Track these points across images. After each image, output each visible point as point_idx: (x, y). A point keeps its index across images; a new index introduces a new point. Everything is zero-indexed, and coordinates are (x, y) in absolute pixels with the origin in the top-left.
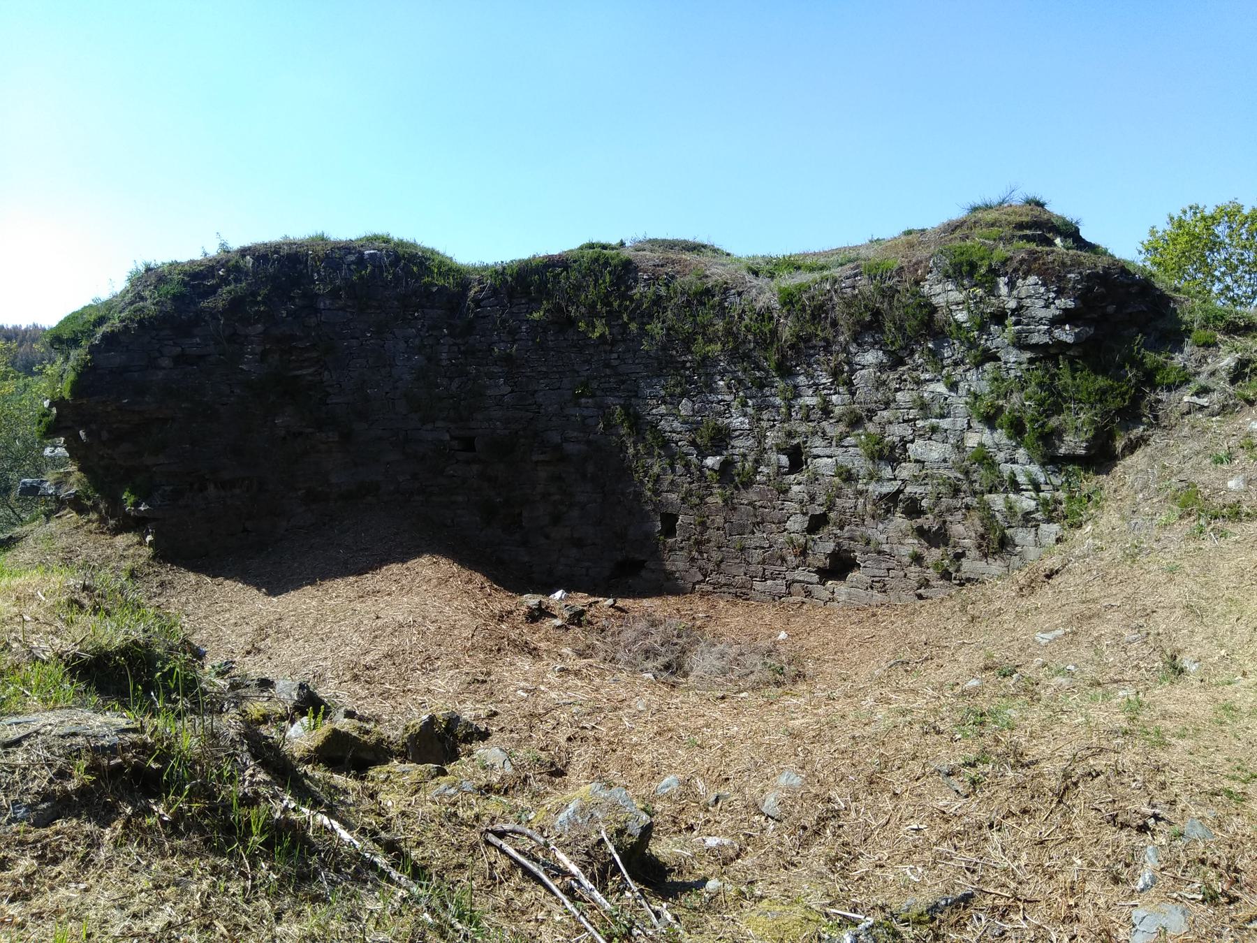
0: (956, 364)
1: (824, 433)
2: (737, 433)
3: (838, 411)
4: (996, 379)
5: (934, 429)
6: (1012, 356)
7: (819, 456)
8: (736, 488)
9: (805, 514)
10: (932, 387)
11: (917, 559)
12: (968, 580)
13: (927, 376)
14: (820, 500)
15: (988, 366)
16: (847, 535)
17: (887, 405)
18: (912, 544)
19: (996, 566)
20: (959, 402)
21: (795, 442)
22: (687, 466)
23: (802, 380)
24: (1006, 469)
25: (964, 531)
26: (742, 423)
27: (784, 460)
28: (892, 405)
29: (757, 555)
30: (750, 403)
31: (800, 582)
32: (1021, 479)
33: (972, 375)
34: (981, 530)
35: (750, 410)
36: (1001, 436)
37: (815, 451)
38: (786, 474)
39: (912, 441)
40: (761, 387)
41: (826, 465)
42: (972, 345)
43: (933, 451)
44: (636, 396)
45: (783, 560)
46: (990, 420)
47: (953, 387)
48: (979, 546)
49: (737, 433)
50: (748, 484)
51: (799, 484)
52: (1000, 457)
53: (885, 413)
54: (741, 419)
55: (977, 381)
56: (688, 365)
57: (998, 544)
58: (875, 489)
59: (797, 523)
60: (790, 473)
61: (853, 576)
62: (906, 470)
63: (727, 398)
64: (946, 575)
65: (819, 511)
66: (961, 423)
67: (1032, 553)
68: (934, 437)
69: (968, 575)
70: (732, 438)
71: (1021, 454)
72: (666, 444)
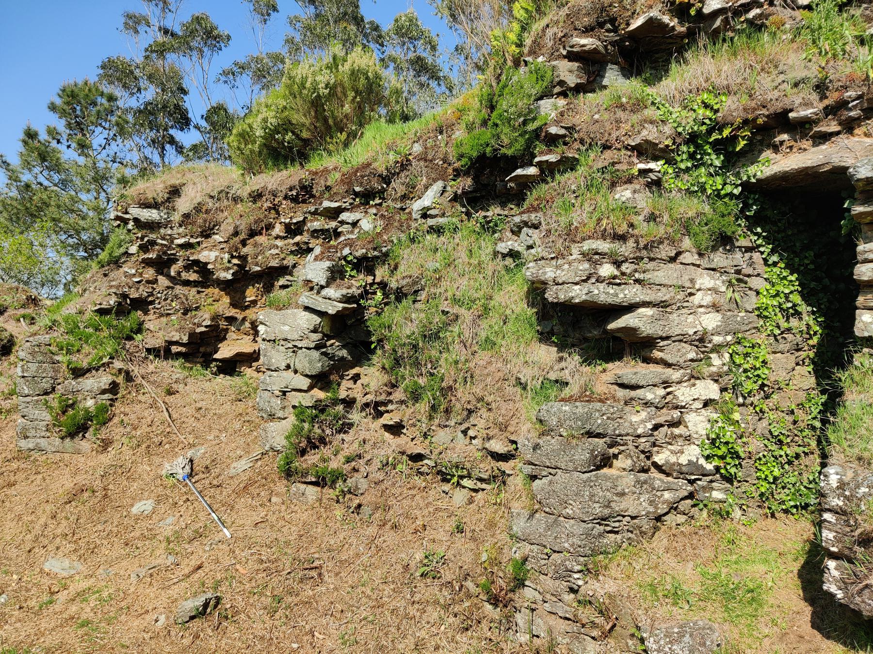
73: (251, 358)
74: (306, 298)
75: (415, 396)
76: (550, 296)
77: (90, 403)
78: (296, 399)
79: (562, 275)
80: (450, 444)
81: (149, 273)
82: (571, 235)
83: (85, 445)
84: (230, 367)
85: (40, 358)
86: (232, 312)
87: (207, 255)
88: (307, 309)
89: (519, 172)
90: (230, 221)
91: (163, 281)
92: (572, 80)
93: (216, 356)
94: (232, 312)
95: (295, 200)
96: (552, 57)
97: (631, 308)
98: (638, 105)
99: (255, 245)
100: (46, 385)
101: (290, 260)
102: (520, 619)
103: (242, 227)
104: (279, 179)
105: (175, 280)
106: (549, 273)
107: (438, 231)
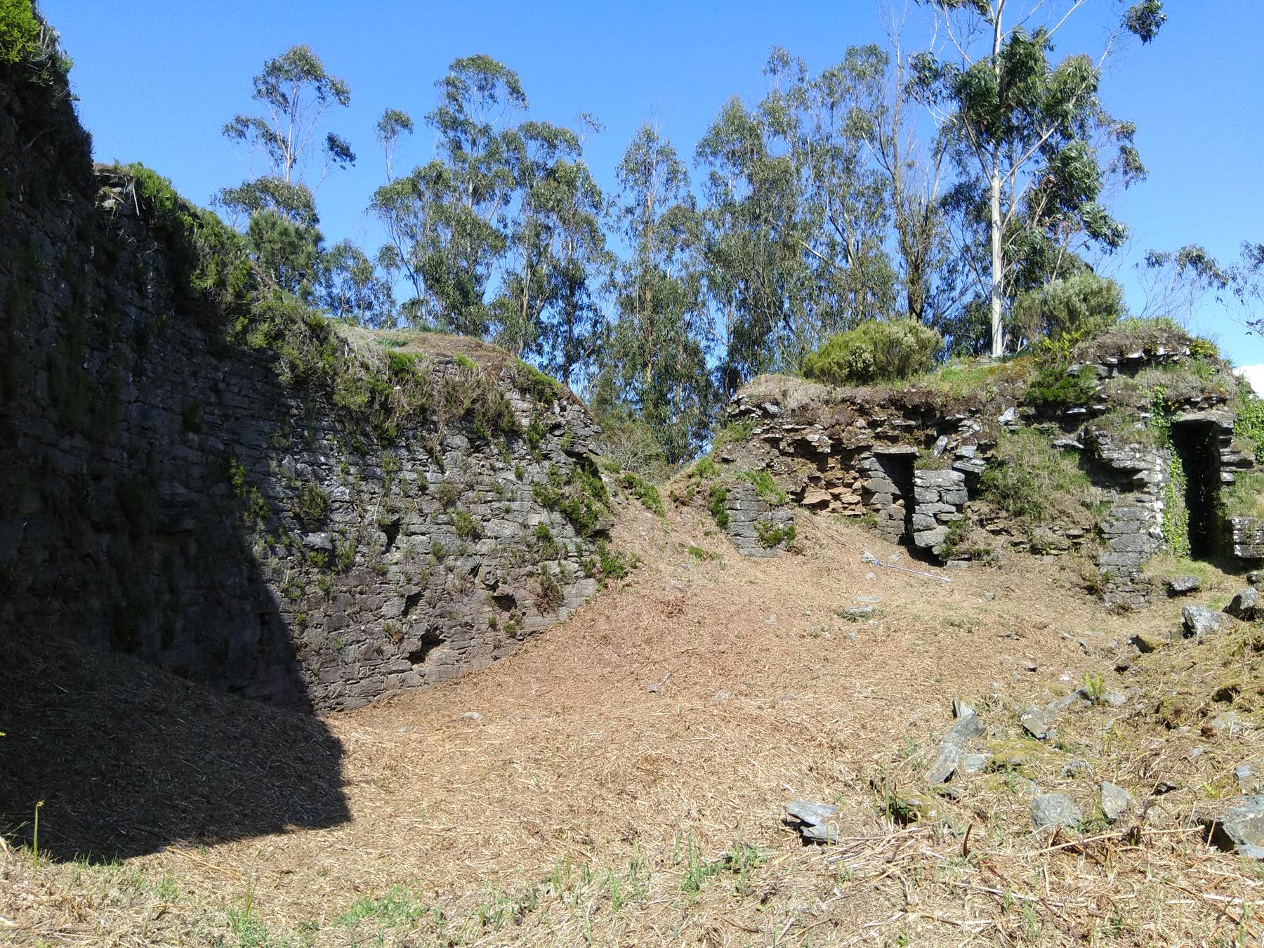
0: (523, 458)
2: (337, 505)
3: (432, 488)
5: (508, 511)
6: (563, 458)
7: (415, 534)
8: (338, 573)
9: (402, 596)
11: (493, 626)
14: (415, 580)
15: (546, 463)
16: (438, 612)
17: (471, 487)
18: (488, 612)
19: (549, 618)
21: (396, 516)
22: (289, 547)
23: (404, 453)
24: (559, 541)
25: (526, 594)
26: (343, 493)
27: (384, 537)
28: (476, 487)
29: (353, 652)
30: (352, 470)
32: (572, 548)
33: (534, 468)
34: (540, 590)
36: (557, 516)
37: (413, 528)
38: (384, 553)
40: (364, 455)
41: (421, 543)
42: (534, 447)
43: (508, 529)
44: (237, 442)
45: (380, 652)
46: (550, 505)
47: (520, 476)
48: (538, 606)
49: (337, 505)
50: (347, 569)
51: (396, 563)
52: (553, 532)
53: (470, 493)
54: (342, 488)
55: (536, 472)
56: (295, 411)
57: (550, 598)
58: (463, 565)
59: (392, 607)
60: (387, 551)
61: (435, 653)
62: (484, 546)
63: (332, 461)
64: (513, 637)
65: (415, 590)
66: (527, 505)
67: (575, 602)
69: (532, 629)
70: (332, 511)
72: (273, 513)
73: (823, 505)
74: (958, 464)
75: (1020, 513)
76: (1115, 465)
77: (781, 526)
78: (944, 517)
79: (1121, 457)
80: (1042, 533)
81: (768, 446)
82: (1125, 441)
83: (780, 550)
84: (814, 507)
85: (750, 498)
86: (818, 474)
87: (813, 437)
88: (954, 469)
89: (1076, 410)
90: (826, 415)
91: (776, 452)
92: (1104, 374)
93: (806, 502)
94: (818, 474)
95: (882, 407)
96: (1094, 362)
97: (1140, 471)
98: (1134, 388)
99: (849, 432)
100: (753, 514)
101: (872, 442)
102: (1106, 597)
103: (842, 420)
104: (863, 393)
105: (783, 453)
106: (1115, 456)
107: (1012, 432)
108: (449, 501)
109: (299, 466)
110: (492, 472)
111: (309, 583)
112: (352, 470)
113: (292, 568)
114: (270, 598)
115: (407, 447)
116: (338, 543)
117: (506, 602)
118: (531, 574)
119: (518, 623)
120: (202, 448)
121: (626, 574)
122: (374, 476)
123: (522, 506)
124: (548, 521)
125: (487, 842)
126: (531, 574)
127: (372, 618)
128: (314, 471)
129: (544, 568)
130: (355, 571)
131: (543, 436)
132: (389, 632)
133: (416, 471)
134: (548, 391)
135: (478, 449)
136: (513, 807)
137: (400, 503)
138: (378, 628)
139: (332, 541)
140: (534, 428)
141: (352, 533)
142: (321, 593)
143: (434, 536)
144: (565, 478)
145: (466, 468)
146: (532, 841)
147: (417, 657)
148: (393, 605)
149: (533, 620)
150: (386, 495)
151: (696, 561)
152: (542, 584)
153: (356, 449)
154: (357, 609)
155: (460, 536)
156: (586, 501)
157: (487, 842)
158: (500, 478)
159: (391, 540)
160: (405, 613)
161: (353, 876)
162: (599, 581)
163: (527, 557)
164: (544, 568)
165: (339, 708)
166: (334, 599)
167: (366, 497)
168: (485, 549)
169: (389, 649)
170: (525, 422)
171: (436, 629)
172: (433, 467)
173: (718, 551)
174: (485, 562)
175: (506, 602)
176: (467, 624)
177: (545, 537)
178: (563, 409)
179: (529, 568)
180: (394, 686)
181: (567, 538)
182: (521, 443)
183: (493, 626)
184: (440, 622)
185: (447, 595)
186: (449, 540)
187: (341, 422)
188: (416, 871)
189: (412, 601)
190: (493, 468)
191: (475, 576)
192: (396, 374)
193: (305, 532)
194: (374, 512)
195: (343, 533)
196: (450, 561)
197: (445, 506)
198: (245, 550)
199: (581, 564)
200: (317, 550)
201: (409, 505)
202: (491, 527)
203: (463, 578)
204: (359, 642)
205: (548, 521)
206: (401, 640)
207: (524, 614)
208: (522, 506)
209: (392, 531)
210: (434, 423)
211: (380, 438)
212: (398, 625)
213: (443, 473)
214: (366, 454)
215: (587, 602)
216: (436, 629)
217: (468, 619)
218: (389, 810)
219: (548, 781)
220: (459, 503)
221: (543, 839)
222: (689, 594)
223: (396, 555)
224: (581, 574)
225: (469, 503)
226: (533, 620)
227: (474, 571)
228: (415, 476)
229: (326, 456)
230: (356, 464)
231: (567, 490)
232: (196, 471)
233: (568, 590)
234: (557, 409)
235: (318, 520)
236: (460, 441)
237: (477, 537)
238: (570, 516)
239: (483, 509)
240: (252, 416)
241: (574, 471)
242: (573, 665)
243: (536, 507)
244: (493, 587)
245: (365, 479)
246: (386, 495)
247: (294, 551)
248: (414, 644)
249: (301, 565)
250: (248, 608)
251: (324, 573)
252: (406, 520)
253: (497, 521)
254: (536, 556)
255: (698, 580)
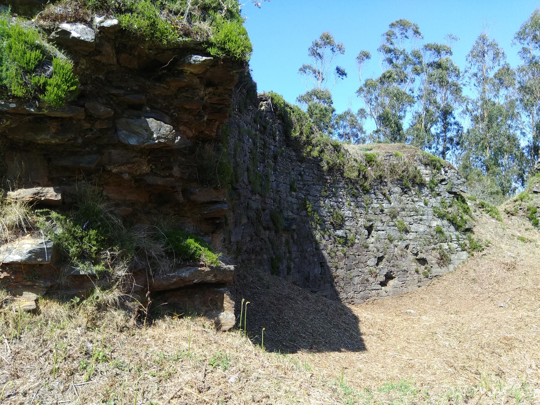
0: (427, 196)
1: (381, 220)
2: (347, 219)
3: (386, 211)
4: (442, 203)
5: (421, 220)
6: (447, 195)
7: (379, 230)
8: (349, 247)
9: (376, 257)
10: (419, 203)
11: (417, 272)
12: (435, 277)
13: (417, 199)
15: (439, 198)
16: (391, 265)
17: (403, 210)
18: (415, 266)
19: (444, 269)
20: (430, 211)
21: (371, 223)
23: (373, 196)
24: (447, 234)
25: (432, 258)
26: (349, 214)
27: (366, 232)
29: (357, 280)
30: (352, 204)
31: (375, 289)
32: (454, 237)
33: (433, 200)
34: (439, 256)
35: (352, 207)
36: (445, 222)
37: (379, 228)
38: (367, 239)
39: (412, 224)
40: (356, 197)
41: (383, 234)
42: (432, 190)
43: (422, 228)
44: (309, 194)
45: (368, 280)
47: (426, 204)
48: (439, 264)
49: (347, 219)
50: (352, 245)
52: (444, 230)
53: (403, 212)
55: (434, 202)
56: (329, 181)
57: (444, 260)
59: (372, 262)
60: (368, 238)
61: (391, 283)
62: (411, 236)
63: (344, 201)
65: (381, 255)
67: (457, 262)
68: (421, 222)
71: (452, 228)
108: (394, 216)
109: (331, 203)
110: (413, 203)
111: (338, 251)
112: (352, 204)
113: (331, 244)
114: (323, 257)
115: (375, 193)
116: (348, 234)
117: (423, 261)
118: (434, 249)
119: (429, 271)
120: (297, 198)
121: (483, 249)
122: (361, 206)
123: (428, 218)
124: (441, 225)
125: (429, 367)
126: (434, 249)
127: (364, 266)
128: (337, 205)
129: (440, 246)
130: (355, 246)
131: (437, 185)
132: (371, 273)
133: (379, 203)
134: (438, 164)
135: (405, 193)
136: (439, 353)
137: (372, 217)
138: (366, 270)
139: (346, 233)
140: (432, 182)
141: (354, 230)
142: (343, 255)
143: (388, 231)
144: (448, 204)
145: (400, 201)
146: (450, 369)
147: (383, 284)
148: (372, 261)
149: (436, 270)
150: (366, 214)
151: (522, 243)
152: (440, 254)
153: (354, 195)
154: (357, 262)
155: (400, 231)
156: (460, 215)
157: (429, 367)
158: (417, 205)
159: (370, 233)
160: (377, 264)
161: (372, 374)
162: (469, 253)
163: (432, 241)
164: (440, 246)
165: (352, 303)
166: (348, 257)
167: (358, 215)
168: (411, 237)
169: (371, 279)
170: (428, 179)
171: (391, 272)
172: (386, 201)
173: (534, 238)
174: (412, 243)
175: (423, 261)
176: (405, 270)
177: (440, 232)
178: (446, 172)
179: (433, 246)
180: (374, 296)
181: (451, 232)
182: (426, 189)
183: (417, 272)
184: (393, 269)
185: (395, 257)
186: (394, 233)
187: (347, 184)
188: (399, 376)
189: (380, 259)
190: (413, 201)
191: (407, 249)
192: (368, 163)
193: (335, 230)
194: (362, 221)
195: (350, 230)
196: (395, 242)
197: (392, 218)
198: (313, 237)
199: (459, 245)
200: (340, 237)
201: (376, 218)
202: (414, 227)
203: (402, 250)
204: (359, 276)
205: (441, 225)
206: (376, 276)
207: (432, 267)
208: (428, 218)
209: (370, 229)
210: (386, 182)
211: (363, 190)
212: (375, 270)
213: (390, 204)
214: (358, 197)
215: (463, 262)
216: (391, 272)
217: (405, 268)
218: (383, 348)
219: (455, 344)
220: (398, 217)
221: (456, 369)
222: (518, 260)
223: (372, 240)
224: (459, 249)
225: (402, 217)
226: (436, 270)
227: (407, 247)
228: (378, 205)
229: (342, 198)
230: (354, 201)
231: (450, 210)
232: (295, 207)
233: (452, 257)
234: (443, 172)
235: (340, 225)
236: (397, 189)
237: (407, 232)
238: (452, 222)
239: (409, 219)
240: (314, 184)
241: (453, 201)
242: (458, 292)
243: (435, 218)
244: (416, 254)
245: (358, 207)
246: (366, 214)
247: (331, 238)
248: (383, 278)
249: (334, 243)
250: (316, 260)
251: (343, 247)
252: (375, 224)
253: (416, 225)
254: (436, 240)
255: (523, 253)
